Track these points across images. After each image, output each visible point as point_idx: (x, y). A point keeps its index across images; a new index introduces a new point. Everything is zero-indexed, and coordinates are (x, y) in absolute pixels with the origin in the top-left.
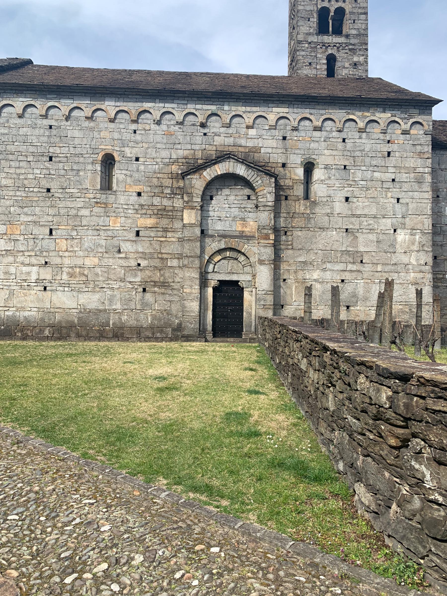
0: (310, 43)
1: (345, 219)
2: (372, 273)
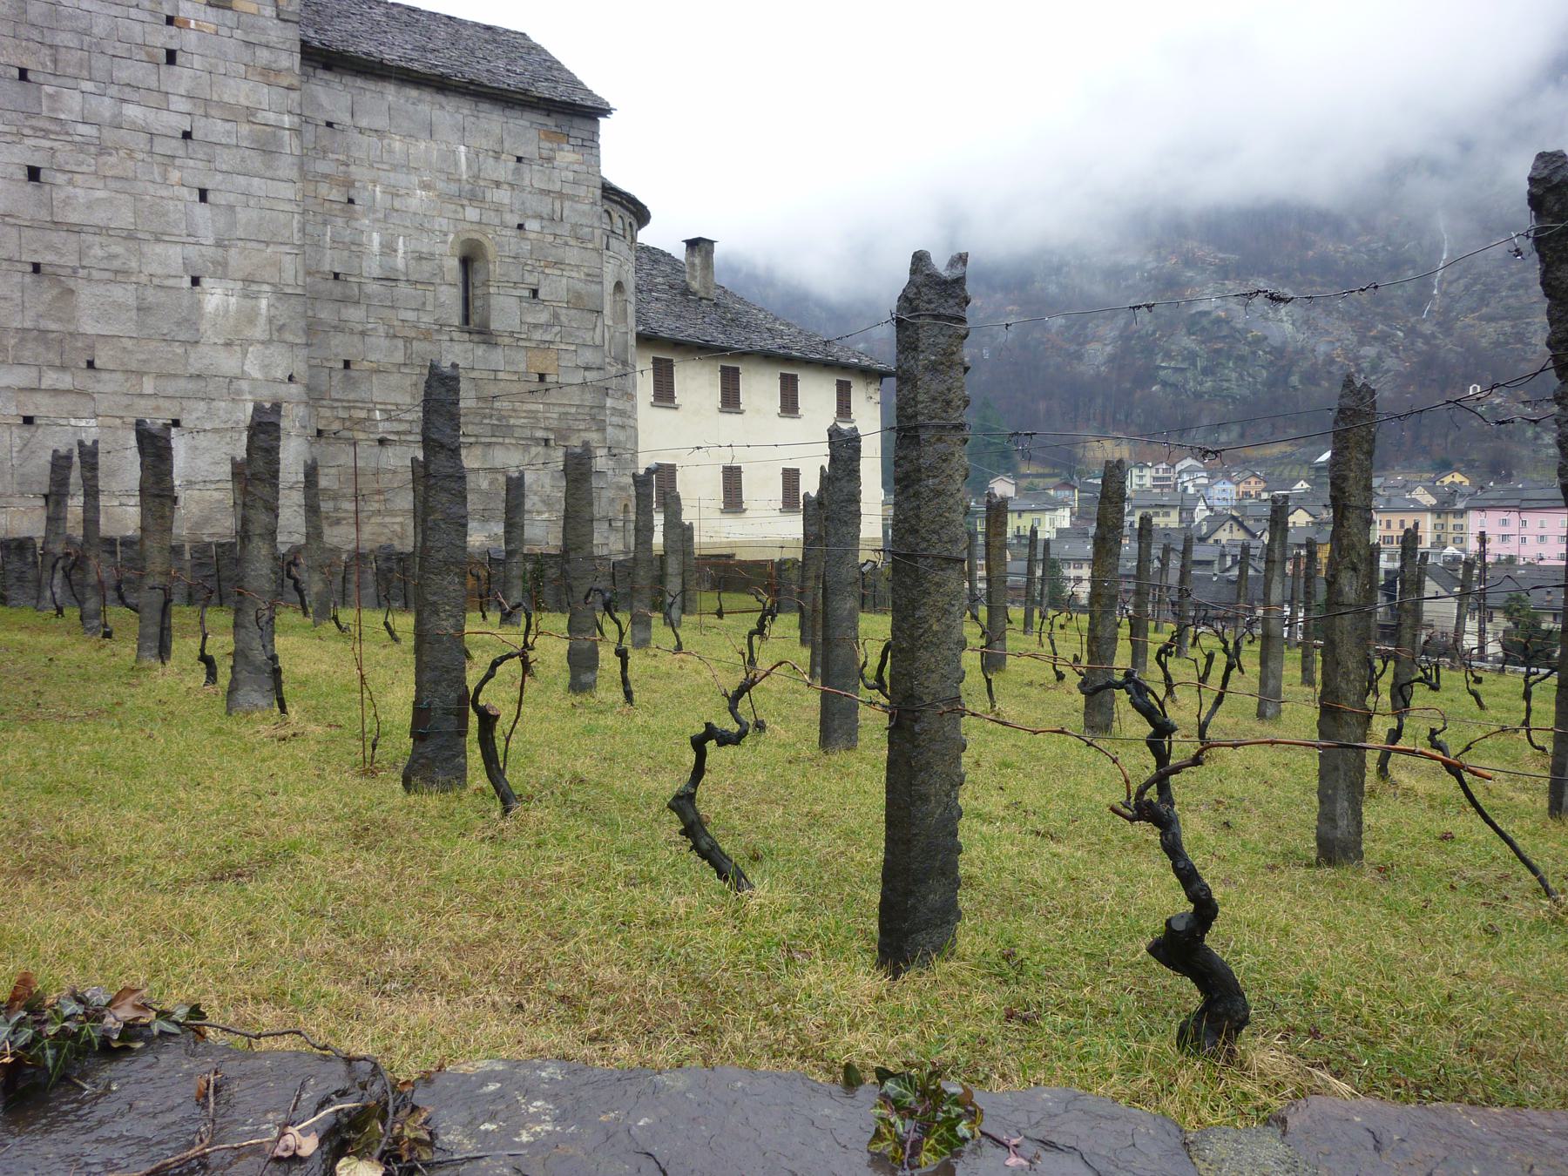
1: (28, 233)
2: (125, 401)
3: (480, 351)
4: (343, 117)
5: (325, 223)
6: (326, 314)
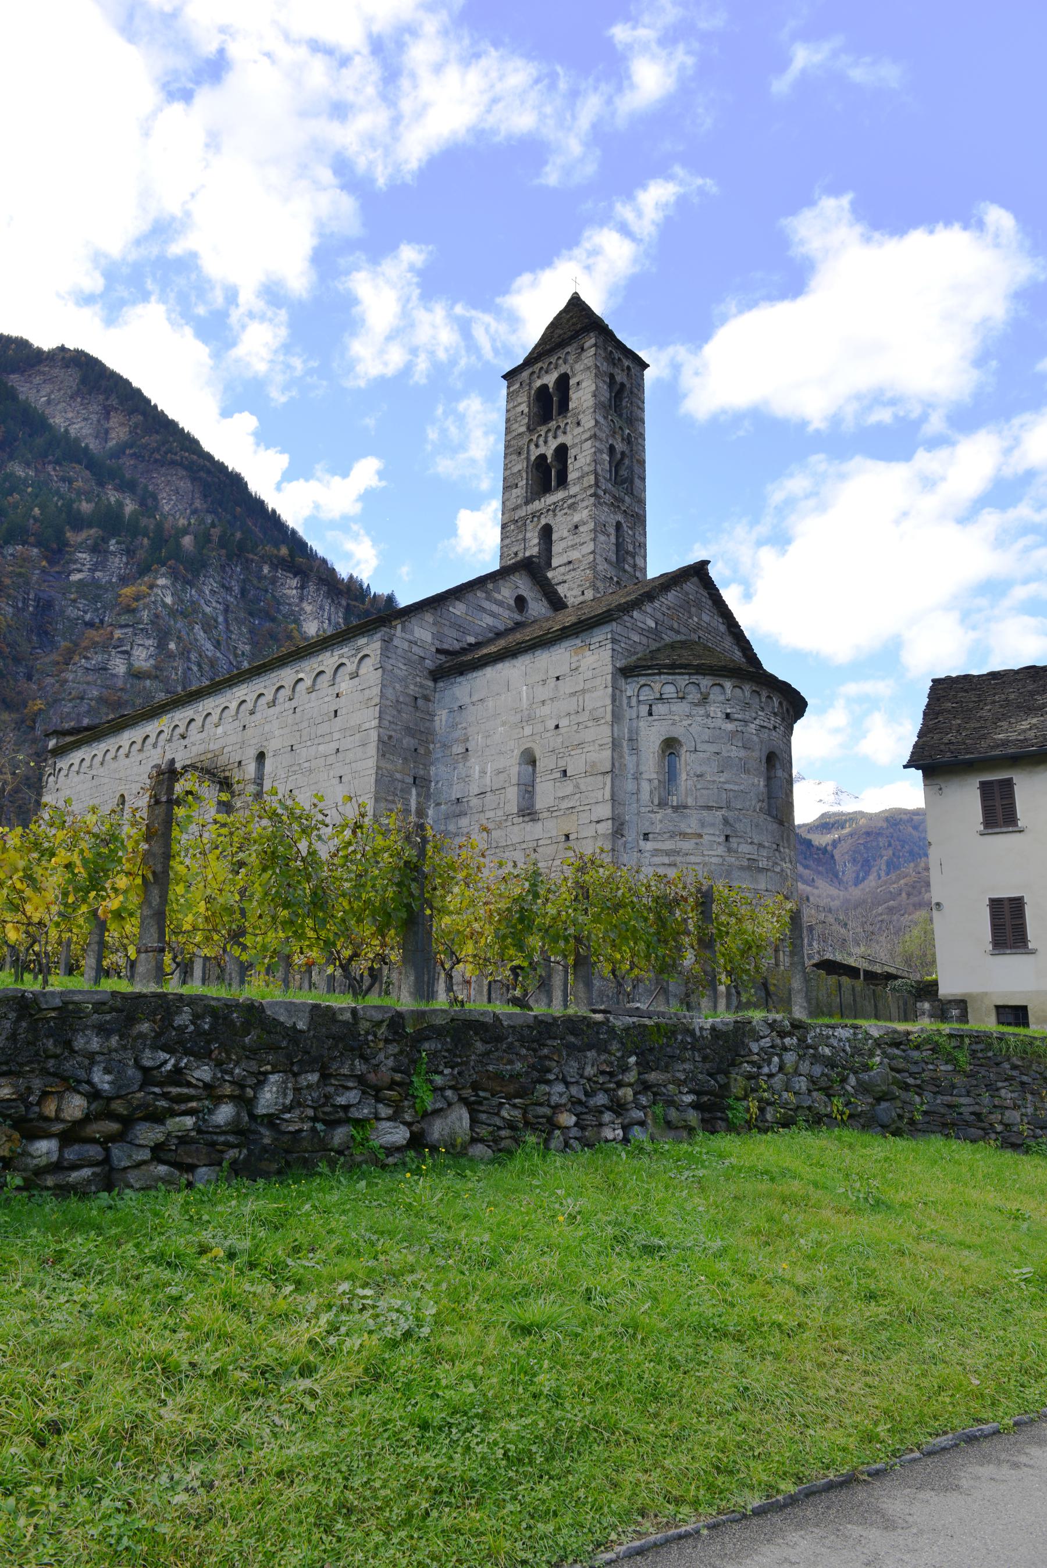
4: (465, 700)
6: (452, 828)
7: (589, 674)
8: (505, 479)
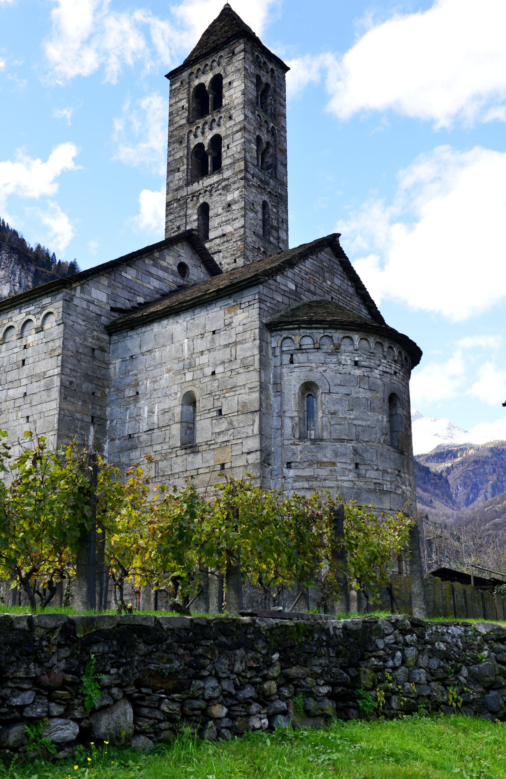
0: (179, 200)
3: (190, 458)
4: (137, 351)
5: (127, 409)
6: (124, 460)
7: (241, 329)
8: (169, 164)
